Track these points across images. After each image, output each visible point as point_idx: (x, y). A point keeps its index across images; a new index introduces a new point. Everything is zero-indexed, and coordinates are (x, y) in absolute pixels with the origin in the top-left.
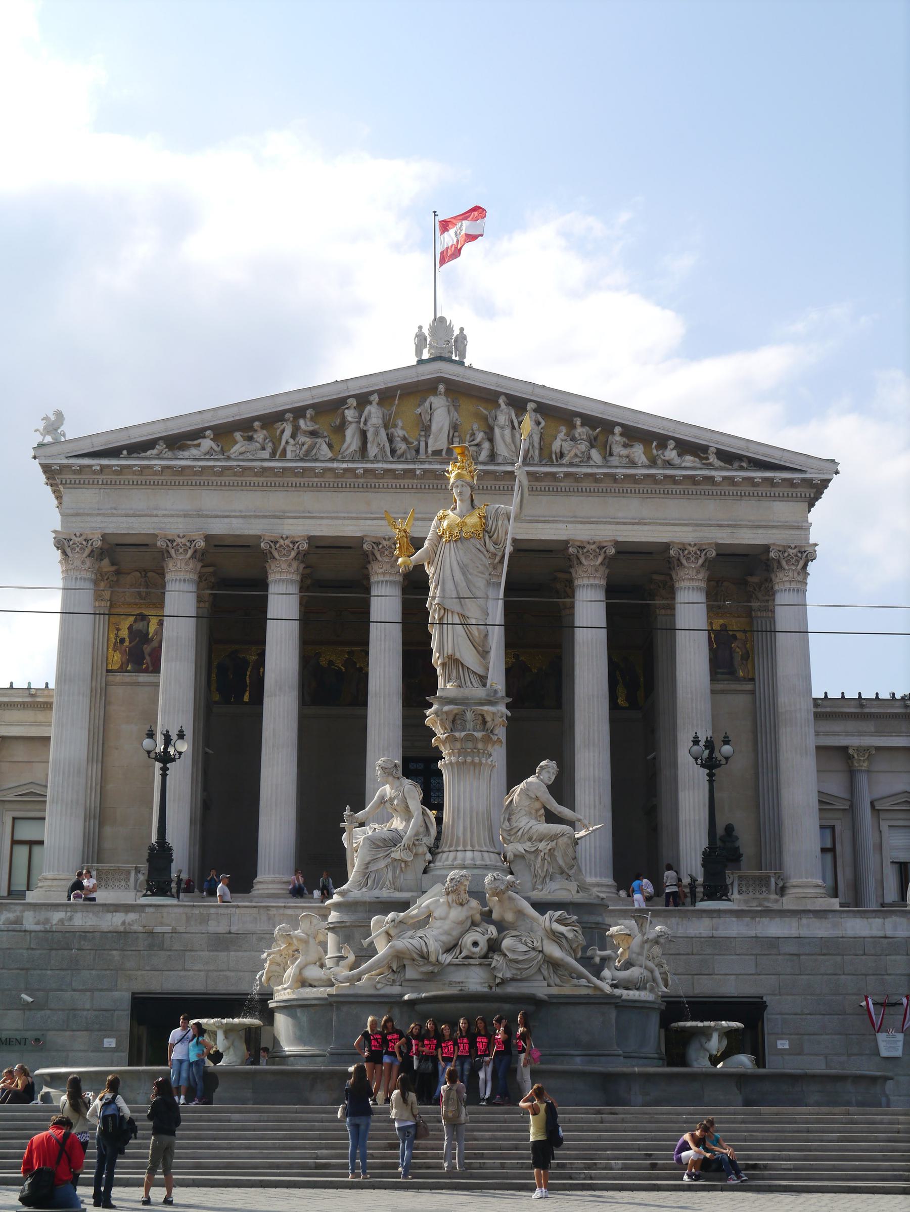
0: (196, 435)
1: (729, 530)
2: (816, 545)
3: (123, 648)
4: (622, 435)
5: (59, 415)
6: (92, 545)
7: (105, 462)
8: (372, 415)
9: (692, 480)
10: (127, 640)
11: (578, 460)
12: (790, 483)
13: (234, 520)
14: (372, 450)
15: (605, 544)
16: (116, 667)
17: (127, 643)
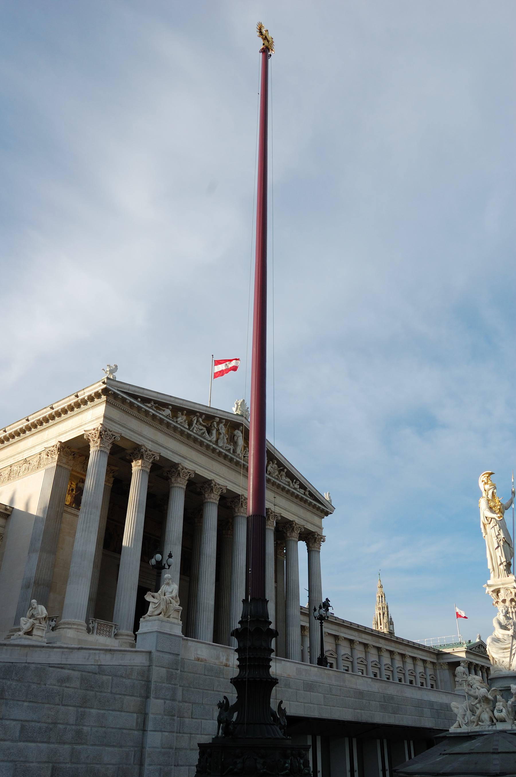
0: (165, 405)
1: (306, 522)
2: (325, 536)
3: (72, 494)
4: (285, 473)
5: (116, 366)
6: (115, 438)
7: (133, 400)
8: (223, 429)
9: (302, 499)
10: (74, 490)
11: (276, 477)
12: (322, 511)
13: (169, 452)
14: (221, 444)
15: (277, 514)
16: (67, 503)
17: (74, 492)
